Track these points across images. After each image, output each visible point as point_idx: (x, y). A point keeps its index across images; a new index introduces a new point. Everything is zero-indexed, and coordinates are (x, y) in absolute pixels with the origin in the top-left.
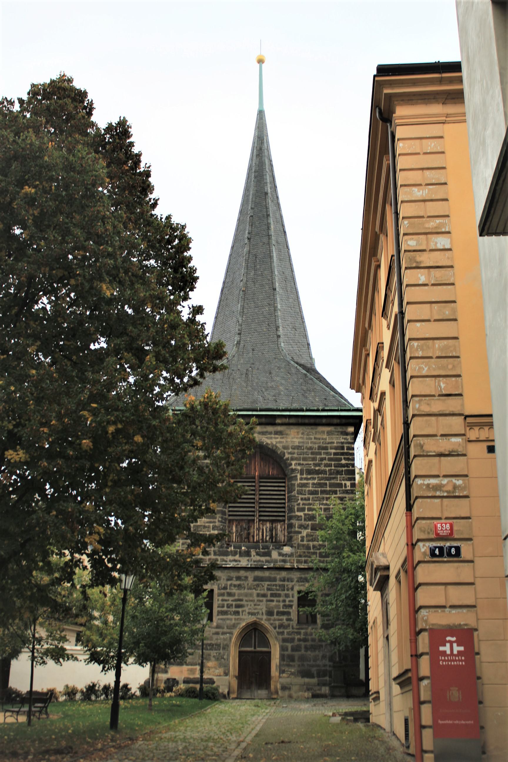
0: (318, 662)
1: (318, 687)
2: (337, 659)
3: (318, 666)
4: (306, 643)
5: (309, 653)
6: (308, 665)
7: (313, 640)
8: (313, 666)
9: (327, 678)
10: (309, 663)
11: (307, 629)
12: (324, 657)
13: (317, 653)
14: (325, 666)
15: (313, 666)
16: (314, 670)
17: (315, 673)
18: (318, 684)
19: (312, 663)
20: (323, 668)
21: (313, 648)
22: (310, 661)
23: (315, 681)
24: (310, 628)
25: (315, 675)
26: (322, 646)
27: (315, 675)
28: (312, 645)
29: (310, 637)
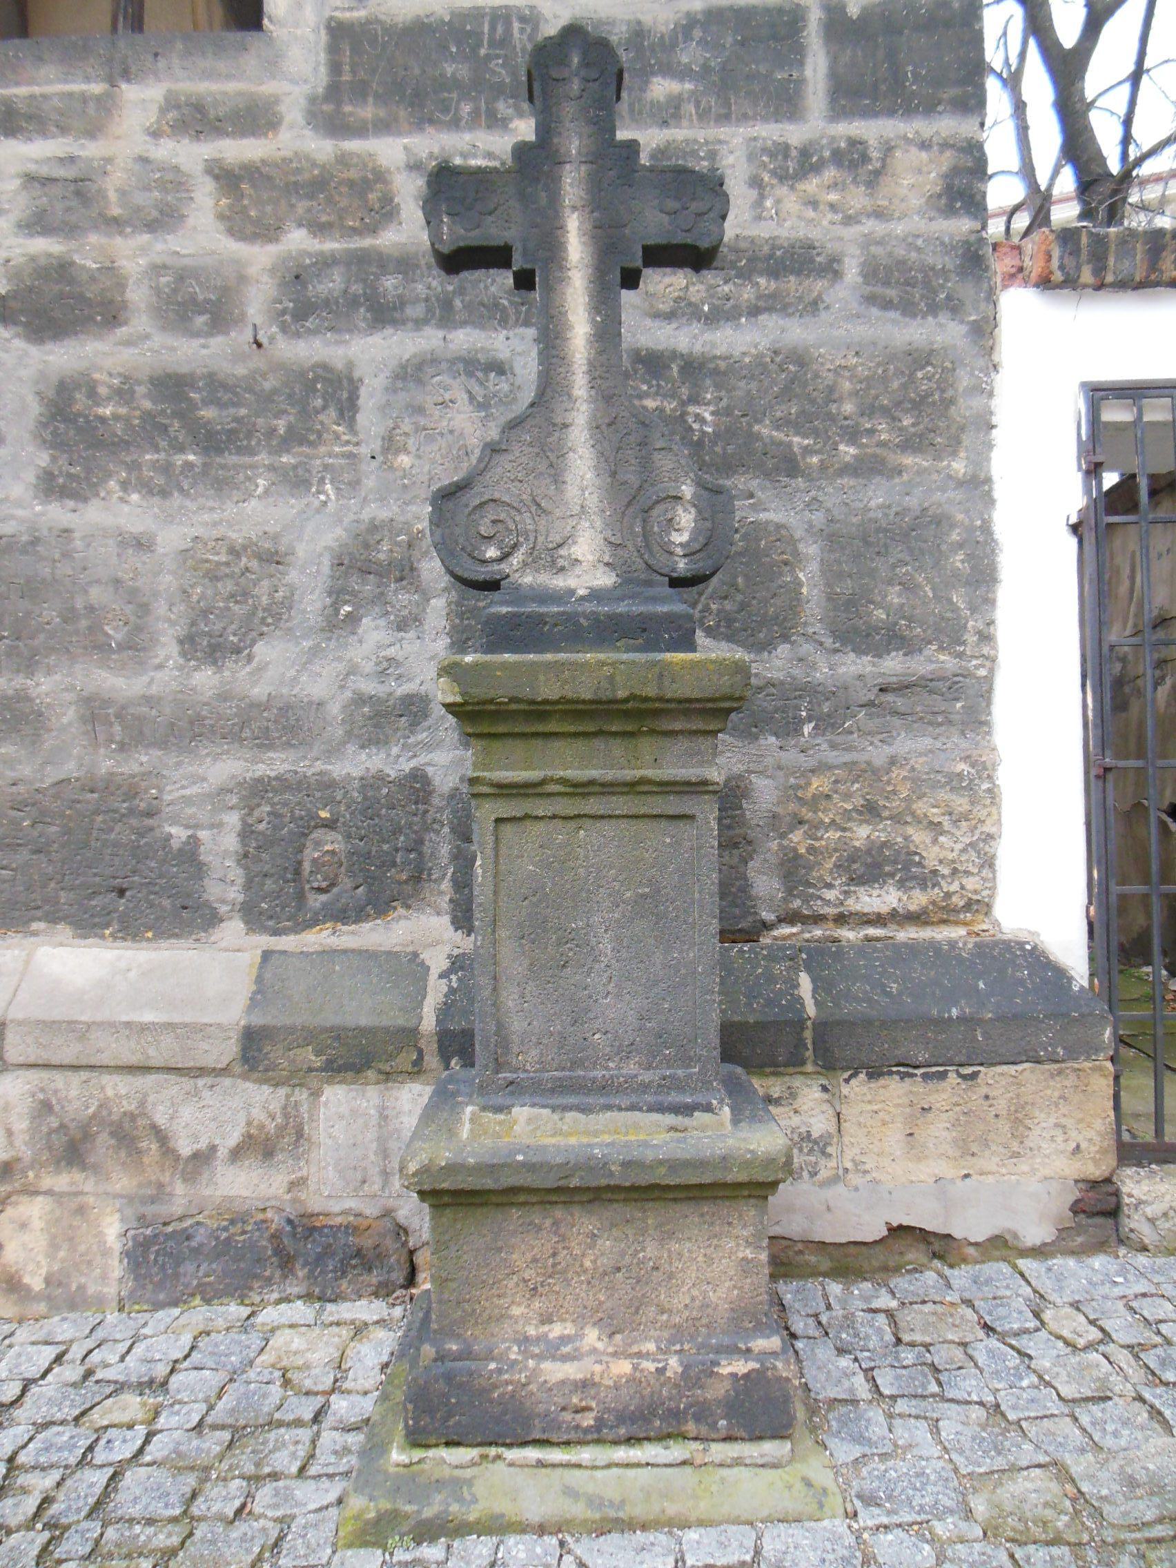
0: (276, 667)
1: (257, 1101)
2: (585, 566)
3: (282, 723)
4: (65, 356)
5: (116, 511)
6: (95, 711)
7: (198, 302)
8: (190, 729)
9: (424, 932)
10: (118, 684)
11: (92, 118)
12: (368, 571)
13: (258, 511)
14: (391, 716)
15: (190, 729)
16: (202, 799)
17: (222, 843)
18: (256, 1051)
19: (166, 675)
20: (355, 764)
21: (193, 427)
22: (136, 647)
23: (210, 976)
24: (141, 100)
25: (225, 884)
26: (340, 390)
27: (225, 884)
28: (172, 386)
29: (134, 255)
